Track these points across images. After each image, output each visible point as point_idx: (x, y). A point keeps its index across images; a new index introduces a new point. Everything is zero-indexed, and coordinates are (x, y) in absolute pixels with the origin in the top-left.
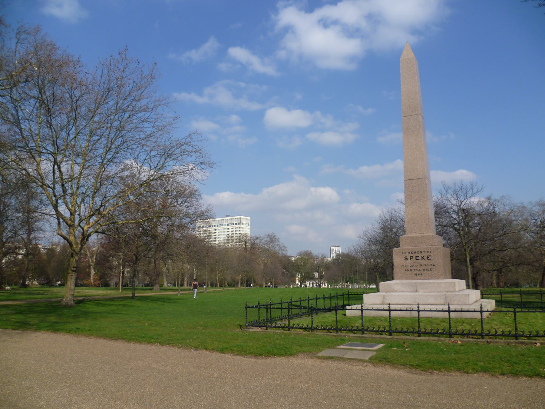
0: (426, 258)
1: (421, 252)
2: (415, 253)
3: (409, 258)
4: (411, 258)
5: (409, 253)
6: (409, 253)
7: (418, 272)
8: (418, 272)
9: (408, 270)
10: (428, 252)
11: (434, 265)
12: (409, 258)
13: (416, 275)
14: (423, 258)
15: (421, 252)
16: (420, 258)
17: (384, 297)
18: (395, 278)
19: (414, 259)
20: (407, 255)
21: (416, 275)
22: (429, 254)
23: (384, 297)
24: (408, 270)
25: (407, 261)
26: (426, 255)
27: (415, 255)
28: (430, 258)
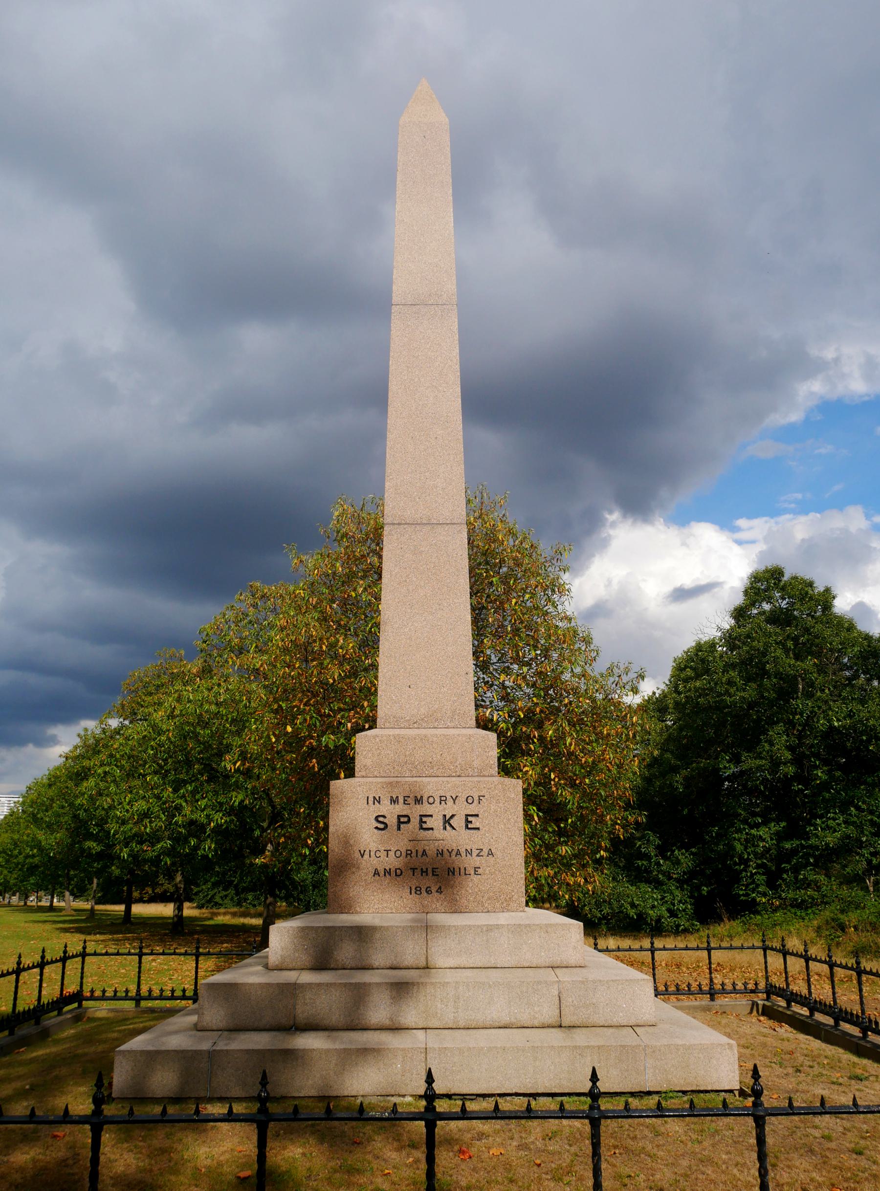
0: (456, 822)
1: (443, 800)
10: (469, 800)
11: (490, 853)
15: (443, 800)
22: (472, 809)
26: (460, 810)
28: (476, 822)
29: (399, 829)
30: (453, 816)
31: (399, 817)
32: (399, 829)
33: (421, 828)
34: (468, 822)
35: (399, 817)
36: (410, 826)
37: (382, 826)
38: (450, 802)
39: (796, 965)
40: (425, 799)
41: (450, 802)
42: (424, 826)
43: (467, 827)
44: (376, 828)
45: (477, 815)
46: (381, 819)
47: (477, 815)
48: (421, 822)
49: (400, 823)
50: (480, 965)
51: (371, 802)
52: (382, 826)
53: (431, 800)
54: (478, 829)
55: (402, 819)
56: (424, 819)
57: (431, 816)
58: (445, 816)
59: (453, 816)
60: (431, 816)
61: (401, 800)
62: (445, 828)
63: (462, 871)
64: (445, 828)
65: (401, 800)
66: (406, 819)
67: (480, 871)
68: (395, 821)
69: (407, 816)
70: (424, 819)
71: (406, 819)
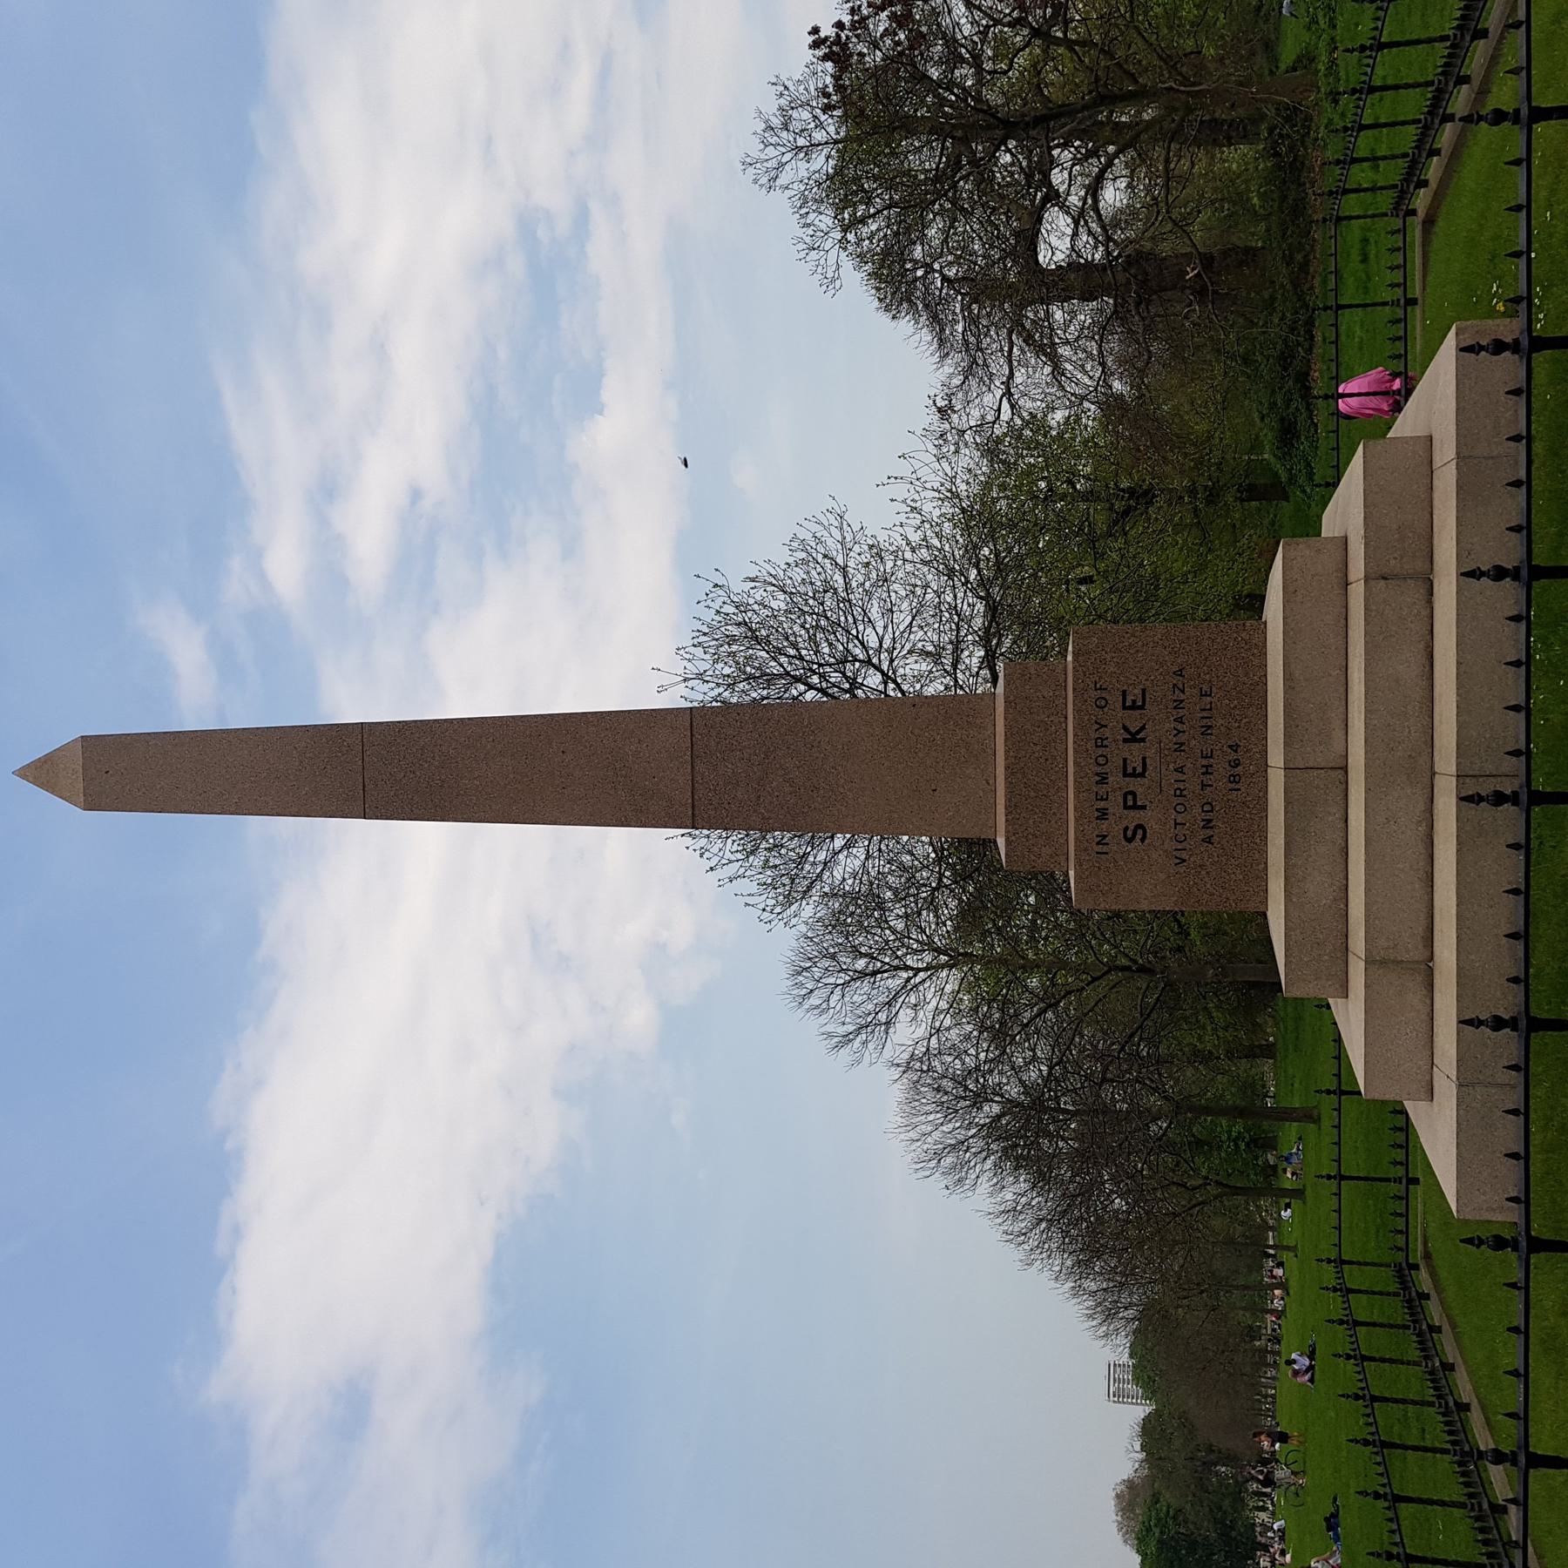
1: (1100, 743)
2: (1103, 779)
3: (1133, 818)
4: (1132, 802)
5: (1103, 814)
6: (1103, 814)
7: (1221, 768)
8: (1221, 768)
9: (1208, 824)
10: (1102, 703)
11: (1180, 673)
12: (1133, 818)
13: (1234, 779)
14: (1133, 738)
15: (1100, 743)
16: (1134, 753)
17: (1383, 963)
18: (1252, 907)
19: (1134, 784)
20: (1113, 826)
21: (1234, 779)
22: (1115, 699)
23: (1383, 963)
24: (1208, 824)
25: (1153, 827)
27: (1115, 779)
28: (1134, 694)
29: (1144, 807)
30: (1125, 728)
31: (1126, 807)
32: (1144, 807)
33: (1142, 775)
34: (1134, 707)
35: (1126, 807)
36: (1139, 791)
37: (1140, 832)
38: (1107, 732)
39: (1361, 175)
40: (1099, 769)
41: (1107, 732)
42: (1139, 770)
43: (1142, 707)
44: (1143, 840)
45: (1124, 692)
46: (1129, 833)
47: (1124, 692)
48: (1134, 775)
49: (1135, 807)
50: (1342, 690)
51: (1105, 849)
52: (1140, 832)
53: (1101, 761)
54: (1144, 691)
55: (1130, 803)
56: (1130, 770)
57: (1125, 760)
58: (1125, 741)
59: (1125, 728)
60: (1125, 760)
61: (1102, 804)
62: (1143, 740)
63: (1205, 714)
64: (1143, 740)
65: (1102, 804)
66: (1130, 797)
67: (1205, 688)
68: (1132, 813)
69: (1125, 795)
70: (1130, 770)
71: (1130, 797)
